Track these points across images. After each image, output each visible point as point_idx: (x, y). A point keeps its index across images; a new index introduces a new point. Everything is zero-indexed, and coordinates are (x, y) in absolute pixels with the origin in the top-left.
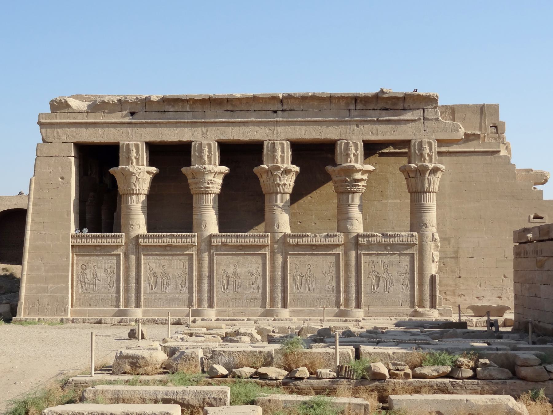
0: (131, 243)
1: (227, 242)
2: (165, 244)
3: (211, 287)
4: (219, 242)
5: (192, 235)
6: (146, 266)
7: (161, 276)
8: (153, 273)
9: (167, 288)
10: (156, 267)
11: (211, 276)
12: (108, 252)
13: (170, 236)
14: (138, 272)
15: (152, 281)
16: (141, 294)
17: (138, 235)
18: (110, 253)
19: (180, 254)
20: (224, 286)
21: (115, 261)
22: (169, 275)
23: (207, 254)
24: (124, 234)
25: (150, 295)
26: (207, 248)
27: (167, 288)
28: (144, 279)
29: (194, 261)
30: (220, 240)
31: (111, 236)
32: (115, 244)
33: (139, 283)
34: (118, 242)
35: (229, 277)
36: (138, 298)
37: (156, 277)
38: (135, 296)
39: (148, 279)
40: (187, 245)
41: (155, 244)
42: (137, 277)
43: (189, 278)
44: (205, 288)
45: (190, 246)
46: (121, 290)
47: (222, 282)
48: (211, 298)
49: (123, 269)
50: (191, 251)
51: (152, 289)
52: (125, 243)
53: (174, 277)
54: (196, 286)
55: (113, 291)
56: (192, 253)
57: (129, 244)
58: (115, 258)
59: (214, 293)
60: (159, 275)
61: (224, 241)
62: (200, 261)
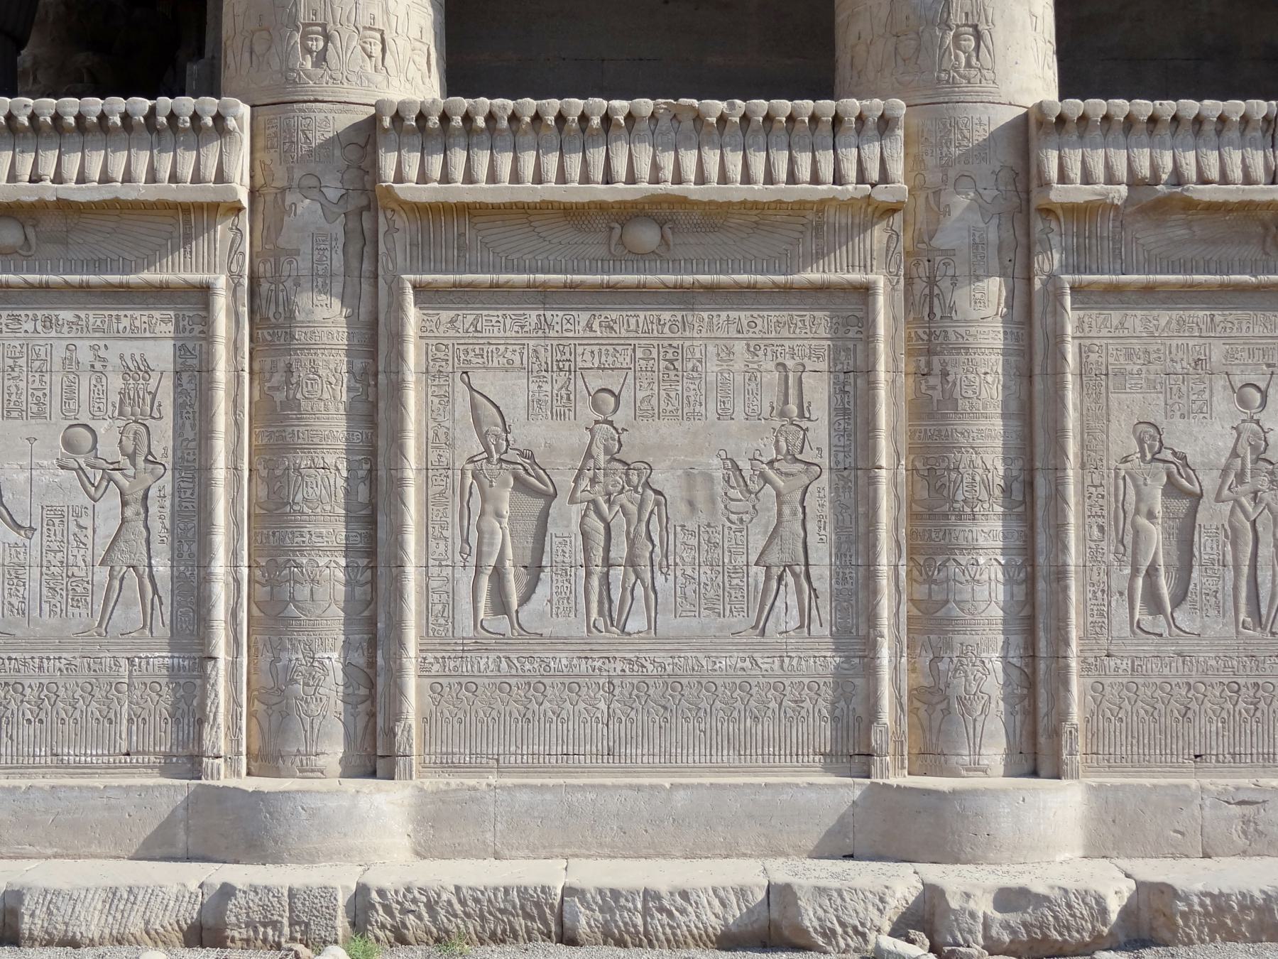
0: (314, 188)
1: (1178, 178)
2: (620, 191)
3: (1031, 581)
4: (1111, 179)
5: (861, 119)
6: (447, 399)
7: (585, 483)
8: (512, 455)
9: (639, 591)
10: (534, 405)
11: (1030, 485)
12: (99, 265)
13: (665, 123)
14: (372, 454)
15: (500, 532)
16: (401, 645)
17: (374, 121)
18: (114, 278)
19: (752, 287)
20: (1152, 572)
21: (162, 354)
22: (658, 479)
23: (994, 288)
24: (245, 110)
25: (486, 661)
26: (993, 236)
27: (639, 591)
28: (426, 505)
29: (882, 347)
30: (1120, 160)
31: (126, 117)
32: (165, 191)
33: (381, 550)
34: (187, 171)
35: (1197, 498)
36: (372, 685)
37: (537, 493)
38: (347, 666)
39: (465, 507)
40: (822, 205)
41: (528, 192)
42: (363, 493)
43: (839, 507)
44: (982, 592)
45: (843, 219)
46: (220, 613)
47: (1128, 539)
48: (1031, 682)
49: (238, 425)
50: (851, 267)
51: (500, 605)
52: (253, 193)
53: (700, 496)
54: (903, 572)
55: (147, 624)
56: (856, 276)
57: (290, 198)
58: (162, 322)
59: (1062, 639)
60: (564, 481)
61: (1155, 168)
62: (930, 352)
